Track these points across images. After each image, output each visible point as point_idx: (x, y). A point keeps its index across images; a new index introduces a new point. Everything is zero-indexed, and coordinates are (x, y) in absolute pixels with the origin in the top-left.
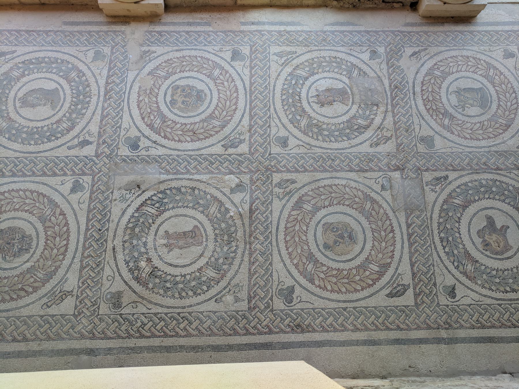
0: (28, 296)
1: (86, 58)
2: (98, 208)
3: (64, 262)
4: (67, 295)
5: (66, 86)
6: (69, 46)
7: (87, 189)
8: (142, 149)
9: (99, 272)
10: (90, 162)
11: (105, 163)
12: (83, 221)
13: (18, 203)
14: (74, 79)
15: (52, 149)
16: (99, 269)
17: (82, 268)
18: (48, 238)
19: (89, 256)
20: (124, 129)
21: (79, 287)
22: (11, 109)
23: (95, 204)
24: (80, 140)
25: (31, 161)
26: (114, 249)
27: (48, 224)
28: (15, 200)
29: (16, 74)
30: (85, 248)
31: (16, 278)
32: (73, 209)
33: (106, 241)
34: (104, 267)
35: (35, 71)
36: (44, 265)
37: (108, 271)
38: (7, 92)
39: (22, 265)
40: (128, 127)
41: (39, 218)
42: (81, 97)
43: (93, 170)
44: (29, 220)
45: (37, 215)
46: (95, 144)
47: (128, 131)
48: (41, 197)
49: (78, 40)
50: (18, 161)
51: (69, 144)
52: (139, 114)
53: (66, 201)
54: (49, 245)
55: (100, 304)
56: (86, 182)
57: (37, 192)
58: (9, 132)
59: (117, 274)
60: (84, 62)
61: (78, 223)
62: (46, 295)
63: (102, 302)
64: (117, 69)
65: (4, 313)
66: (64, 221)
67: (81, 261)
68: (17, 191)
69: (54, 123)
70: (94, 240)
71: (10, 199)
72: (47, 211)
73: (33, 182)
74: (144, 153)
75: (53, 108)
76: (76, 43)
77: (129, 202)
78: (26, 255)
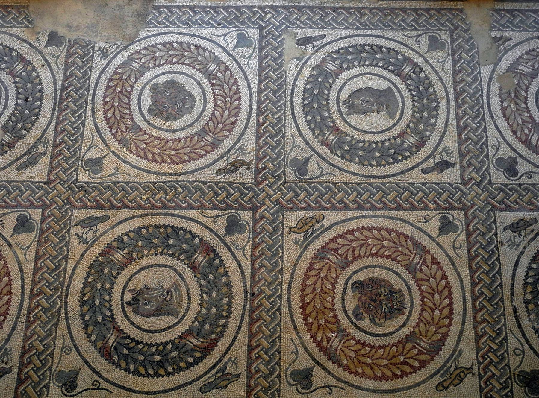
0: (416, 373)
1: (419, 47)
2: (482, 255)
3: (452, 328)
4: (466, 372)
5: (402, 86)
6: (393, 29)
7: (460, 228)
8: (522, 175)
9: (501, 342)
10: (457, 192)
11: (477, 194)
12: (465, 272)
13: (374, 246)
14: (410, 76)
15: (402, 173)
16: (500, 339)
17: (478, 338)
18: (424, 294)
19: (484, 320)
20: (492, 147)
21: (479, 363)
22: (336, 116)
23: (476, 250)
24: (436, 161)
25: (378, 188)
26: (515, 311)
27: (419, 275)
28: (369, 241)
29: (332, 68)
30: (476, 311)
31: (394, 348)
32: (448, 255)
33: (502, 300)
34: (507, 337)
35: (356, 63)
36: (427, 331)
37: (513, 343)
38: (326, 92)
39: (397, 330)
40: (496, 143)
41: (407, 267)
42: (425, 101)
43: (464, 204)
44: (394, 269)
45: (403, 263)
46: (458, 165)
47: (498, 149)
48: (402, 239)
49: (403, 20)
50: (360, 188)
51: (422, 167)
52: (507, 126)
53: (437, 244)
54: (427, 304)
55: (512, 387)
56: (458, 219)
57: (396, 231)
58: (341, 148)
59: (526, 347)
60: (417, 52)
61: (459, 275)
62: (438, 371)
63: (514, 384)
64: (464, 62)
65: (389, 394)
66: (440, 273)
67: (475, 328)
68: (370, 229)
69: (397, 137)
70: (485, 298)
71: (362, 240)
72: (414, 257)
73: (388, 217)
74: (525, 180)
75: (391, 115)
76: (400, 25)
77: (521, 248)
78: (401, 317)
